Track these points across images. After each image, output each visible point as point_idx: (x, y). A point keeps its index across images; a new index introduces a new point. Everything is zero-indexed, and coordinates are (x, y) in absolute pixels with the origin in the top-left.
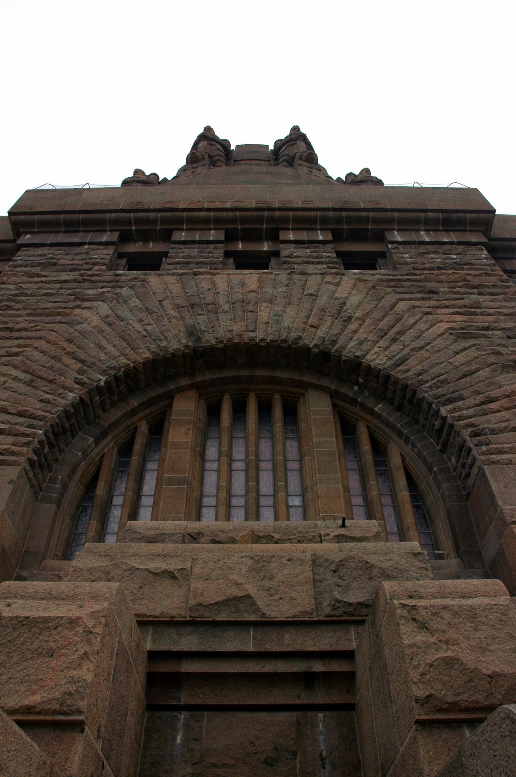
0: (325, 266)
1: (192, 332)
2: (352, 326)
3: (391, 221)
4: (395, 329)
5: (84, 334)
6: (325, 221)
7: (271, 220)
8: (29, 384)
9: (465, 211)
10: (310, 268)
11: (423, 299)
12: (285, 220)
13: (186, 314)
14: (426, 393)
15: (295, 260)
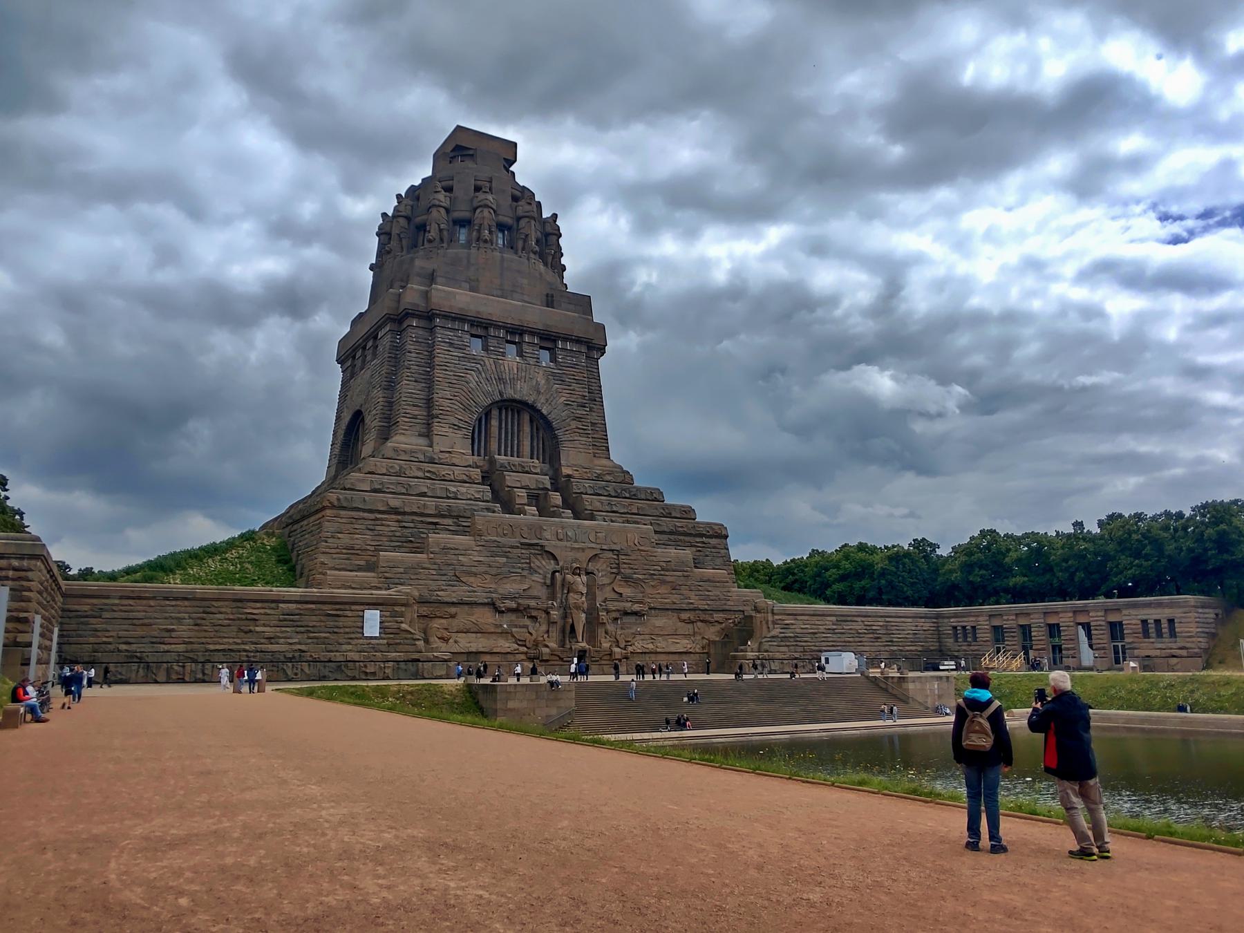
10: (532, 361)
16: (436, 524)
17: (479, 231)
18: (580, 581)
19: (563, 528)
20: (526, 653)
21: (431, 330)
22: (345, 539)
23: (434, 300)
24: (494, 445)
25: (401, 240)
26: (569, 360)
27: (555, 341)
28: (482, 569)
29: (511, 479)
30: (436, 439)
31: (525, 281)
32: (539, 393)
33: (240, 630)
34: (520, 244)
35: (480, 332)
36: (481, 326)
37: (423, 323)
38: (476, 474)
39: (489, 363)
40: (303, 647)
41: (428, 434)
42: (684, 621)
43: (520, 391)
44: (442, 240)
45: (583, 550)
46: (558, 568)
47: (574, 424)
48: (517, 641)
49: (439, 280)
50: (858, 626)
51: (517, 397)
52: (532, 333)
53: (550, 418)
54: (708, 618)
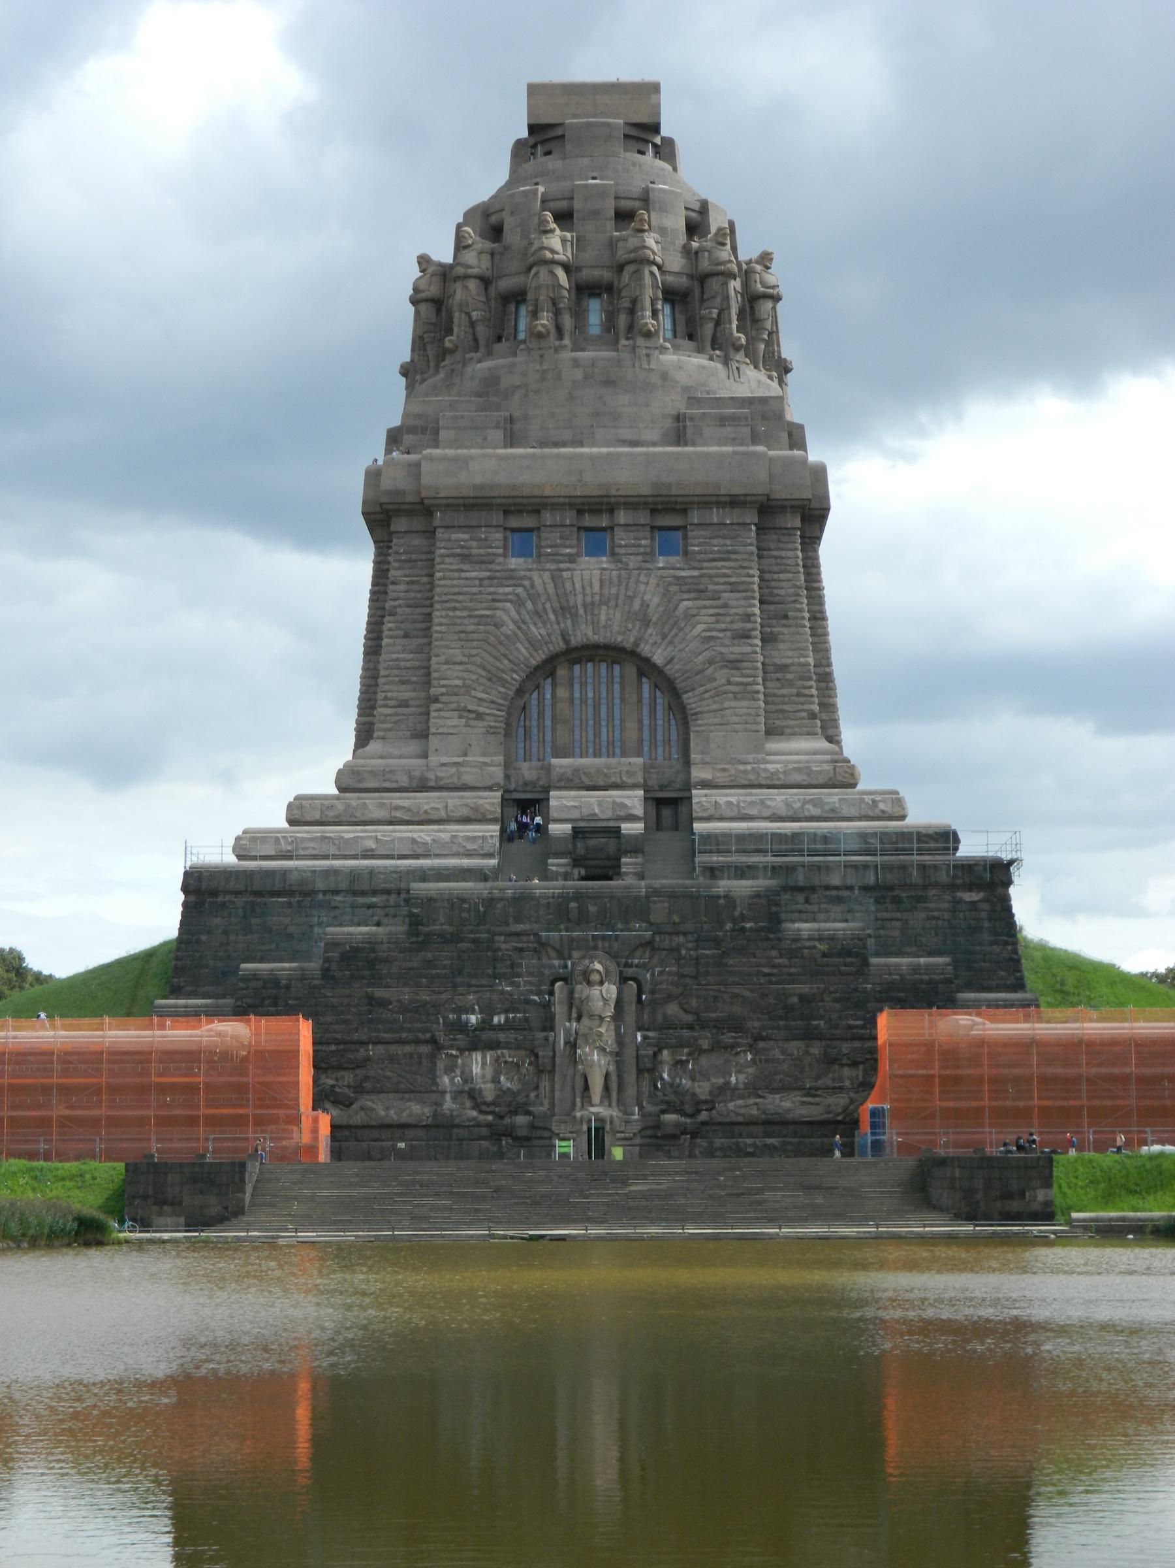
0: (640, 558)
1: (565, 637)
2: (650, 631)
3: (692, 503)
4: (672, 633)
5: (507, 637)
6: (646, 503)
7: (608, 503)
8: (490, 679)
9: (746, 495)
10: (633, 562)
11: (695, 599)
12: (618, 504)
13: (560, 618)
14: (680, 685)
15: (622, 551)
17: (535, 314)
20: (488, 1125)
21: (431, 533)
23: (425, 480)
25: (425, 350)
26: (716, 546)
27: (684, 511)
29: (559, 800)
30: (434, 742)
32: (646, 622)
34: (623, 320)
35: (527, 521)
36: (518, 514)
37: (418, 523)
38: (491, 801)
39: (541, 580)
41: (423, 734)
43: (610, 626)
44: (476, 340)
47: (722, 676)
49: (443, 434)
51: (601, 638)
52: (633, 504)
53: (669, 670)
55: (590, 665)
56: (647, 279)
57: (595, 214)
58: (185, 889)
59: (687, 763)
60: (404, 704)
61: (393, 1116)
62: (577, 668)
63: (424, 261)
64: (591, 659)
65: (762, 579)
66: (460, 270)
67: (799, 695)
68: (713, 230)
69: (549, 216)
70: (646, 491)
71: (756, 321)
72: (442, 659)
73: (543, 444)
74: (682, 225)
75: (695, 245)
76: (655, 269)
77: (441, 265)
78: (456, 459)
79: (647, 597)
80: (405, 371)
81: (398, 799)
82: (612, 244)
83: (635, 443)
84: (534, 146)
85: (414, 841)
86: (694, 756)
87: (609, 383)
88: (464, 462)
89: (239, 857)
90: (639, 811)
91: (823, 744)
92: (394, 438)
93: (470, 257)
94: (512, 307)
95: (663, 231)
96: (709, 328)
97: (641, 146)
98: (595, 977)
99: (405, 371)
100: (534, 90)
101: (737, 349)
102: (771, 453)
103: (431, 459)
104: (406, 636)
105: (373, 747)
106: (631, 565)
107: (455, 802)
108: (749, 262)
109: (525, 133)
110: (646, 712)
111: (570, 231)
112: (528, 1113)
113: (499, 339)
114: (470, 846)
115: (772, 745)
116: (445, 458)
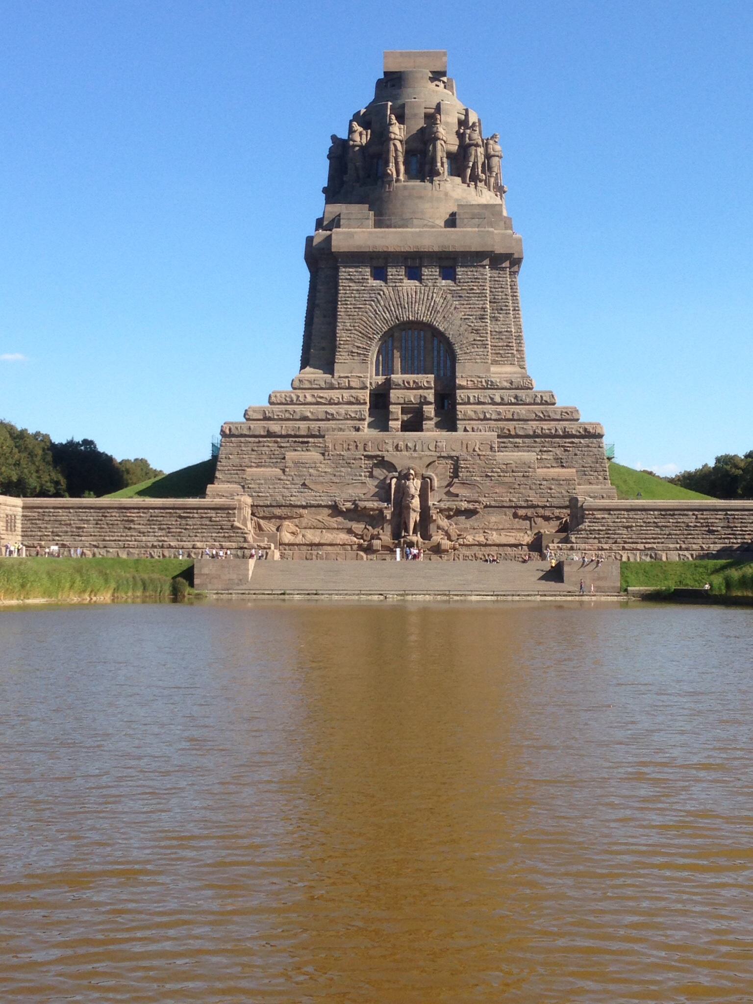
14: (452, 340)
16: (308, 442)
18: (414, 486)
19: (404, 441)
21: (336, 270)
22: (234, 459)
23: (334, 243)
24: (398, 364)
28: (327, 478)
29: (394, 394)
31: (427, 205)
33: (126, 528)
38: (365, 395)
40: (166, 539)
42: (520, 517)
45: (421, 458)
46: (396, 474)
47: (472, 337)
48: (356, 535)
49: (342, 222)
50: (691, 520)
54: (548, 513)
55: (410, 332)
56: (439, 147)
57: (415, 115)
58: (223, 434)
59: (453, 377)
60: (323, 349)
61: (317, 541)
62: (404, 333)
63: (334, 138)
64: (410, 329)
65: (491, 292)
66: (351, 143)
67: (507, 346)
68: (470, 124)
69: (393, 117)
70: (436, 249)
71: (490, 169)
72: (341, 328)
73: (389, 227)
74: (456, 121)
75: (462, 131)
76: (443, 142)
77: (341, 139)
78: (348, 233)
79: (437, 300)
80: (325, 190)
81: (321, 393)
82: (422, 130)
83: (433, 227)
84: (387, 82)
85: (326, 412)
86: (458, 374)
87: (421, 197)
88: (351, 235)
89: (248, 419)
90: (433, 400)
91: (517, 369)
92: (319, 224)
93: (357, 137)
94: (375, 161)
95: (447, 124)
96: (469, 171)
97: (437, 83)
98: (412, 477)
99: (325, 190)
100: (386, 55)
101: (481, 181)
102: (496, 231)
103: (337, 233)
104: (325, 316)
105: (308, 369)
106: (430, 284)
107: (346, 395)
108: (487, 139)
109: (383, 77)
110: (436, 353)
111: (403, 124)
112: (380, 539)
113: (369, 177)
114: (353, 415)
115: (494, 369)
116: (344, 233)
